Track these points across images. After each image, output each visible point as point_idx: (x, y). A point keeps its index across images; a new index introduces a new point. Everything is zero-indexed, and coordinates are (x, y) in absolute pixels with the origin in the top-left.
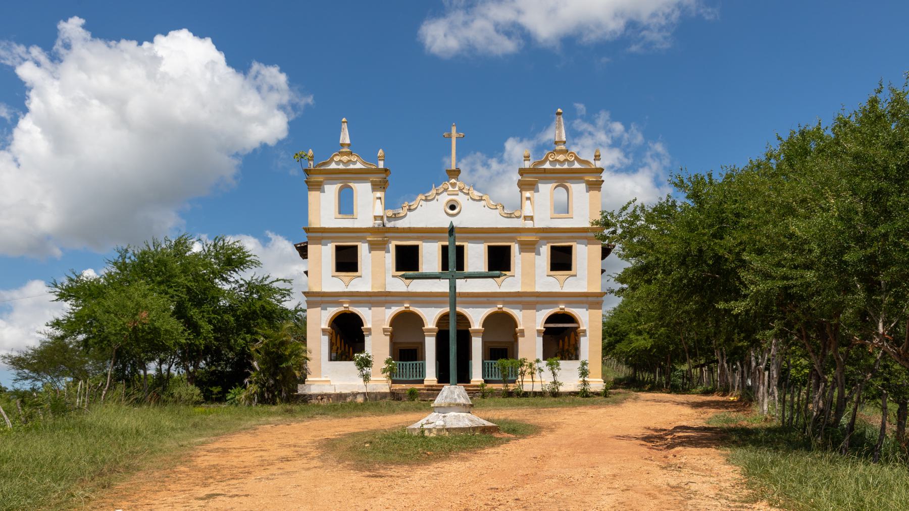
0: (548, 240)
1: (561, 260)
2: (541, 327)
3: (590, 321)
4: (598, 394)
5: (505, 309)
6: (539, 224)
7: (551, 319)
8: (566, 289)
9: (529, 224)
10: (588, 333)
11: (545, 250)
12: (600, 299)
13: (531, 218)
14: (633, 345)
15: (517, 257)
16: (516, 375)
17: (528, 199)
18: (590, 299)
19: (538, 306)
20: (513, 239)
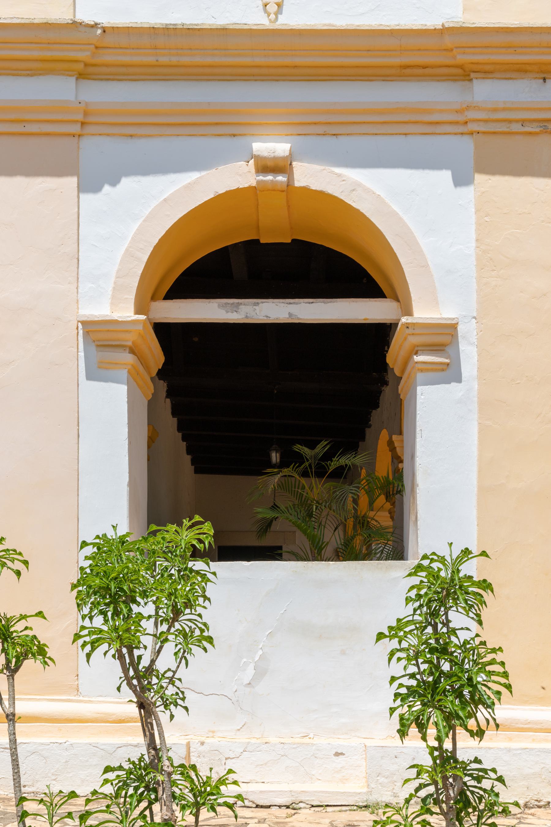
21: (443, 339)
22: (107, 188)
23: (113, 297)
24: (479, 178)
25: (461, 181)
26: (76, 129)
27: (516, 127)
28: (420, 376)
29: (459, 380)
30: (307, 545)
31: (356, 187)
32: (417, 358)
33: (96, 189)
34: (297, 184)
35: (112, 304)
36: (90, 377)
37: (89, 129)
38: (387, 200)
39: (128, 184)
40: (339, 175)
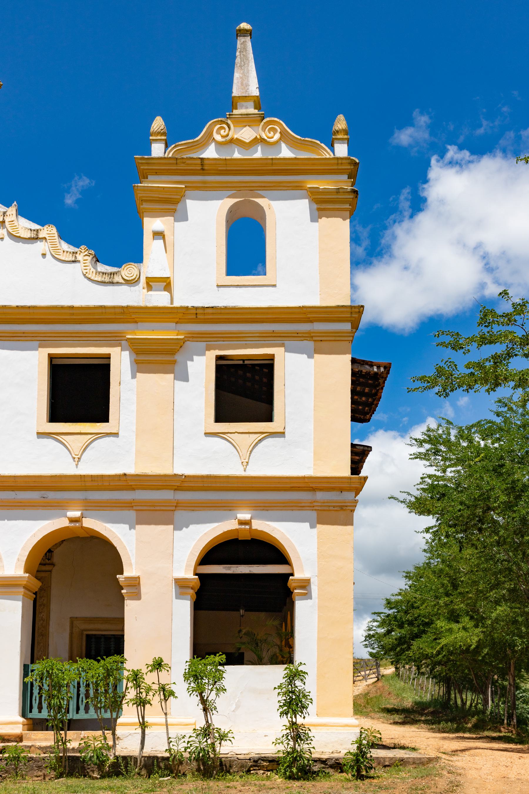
0: (209, 340)
1: (245, 392)
2: (185, 568)
3: (321, 556)
4: (338, 766)
5: (89, 523)
6: (184, 297)
7: (217, 552)
8: (256, 470)
9: (159, 299)
10: (314, 588)
11: (202, 369)
12: (349, 496)
13: (166, 284)
14: (443, 641)
15: (126, 386)
16: (116, 705)
17: (159, 235)
18: (320, 496)
19: (179, 515)
20: (115, 339)
21: (305, 584)
22: (184, 529)
23: (186, 569)
24: (318, 526)
25: (312, 526)
26: (174, 508)
27: (331, 508)
28: (297, 597)
29: (311, 598)
30: (256, 658)
31: (274, 529)
32: (295, 591)
33: (180, 529)
34: (253, 528)
35: (185, 571)
36: (176, 598)
37: (178, 508)
38: (286, 534)
39: (192, 527)
40: (268, 525)
